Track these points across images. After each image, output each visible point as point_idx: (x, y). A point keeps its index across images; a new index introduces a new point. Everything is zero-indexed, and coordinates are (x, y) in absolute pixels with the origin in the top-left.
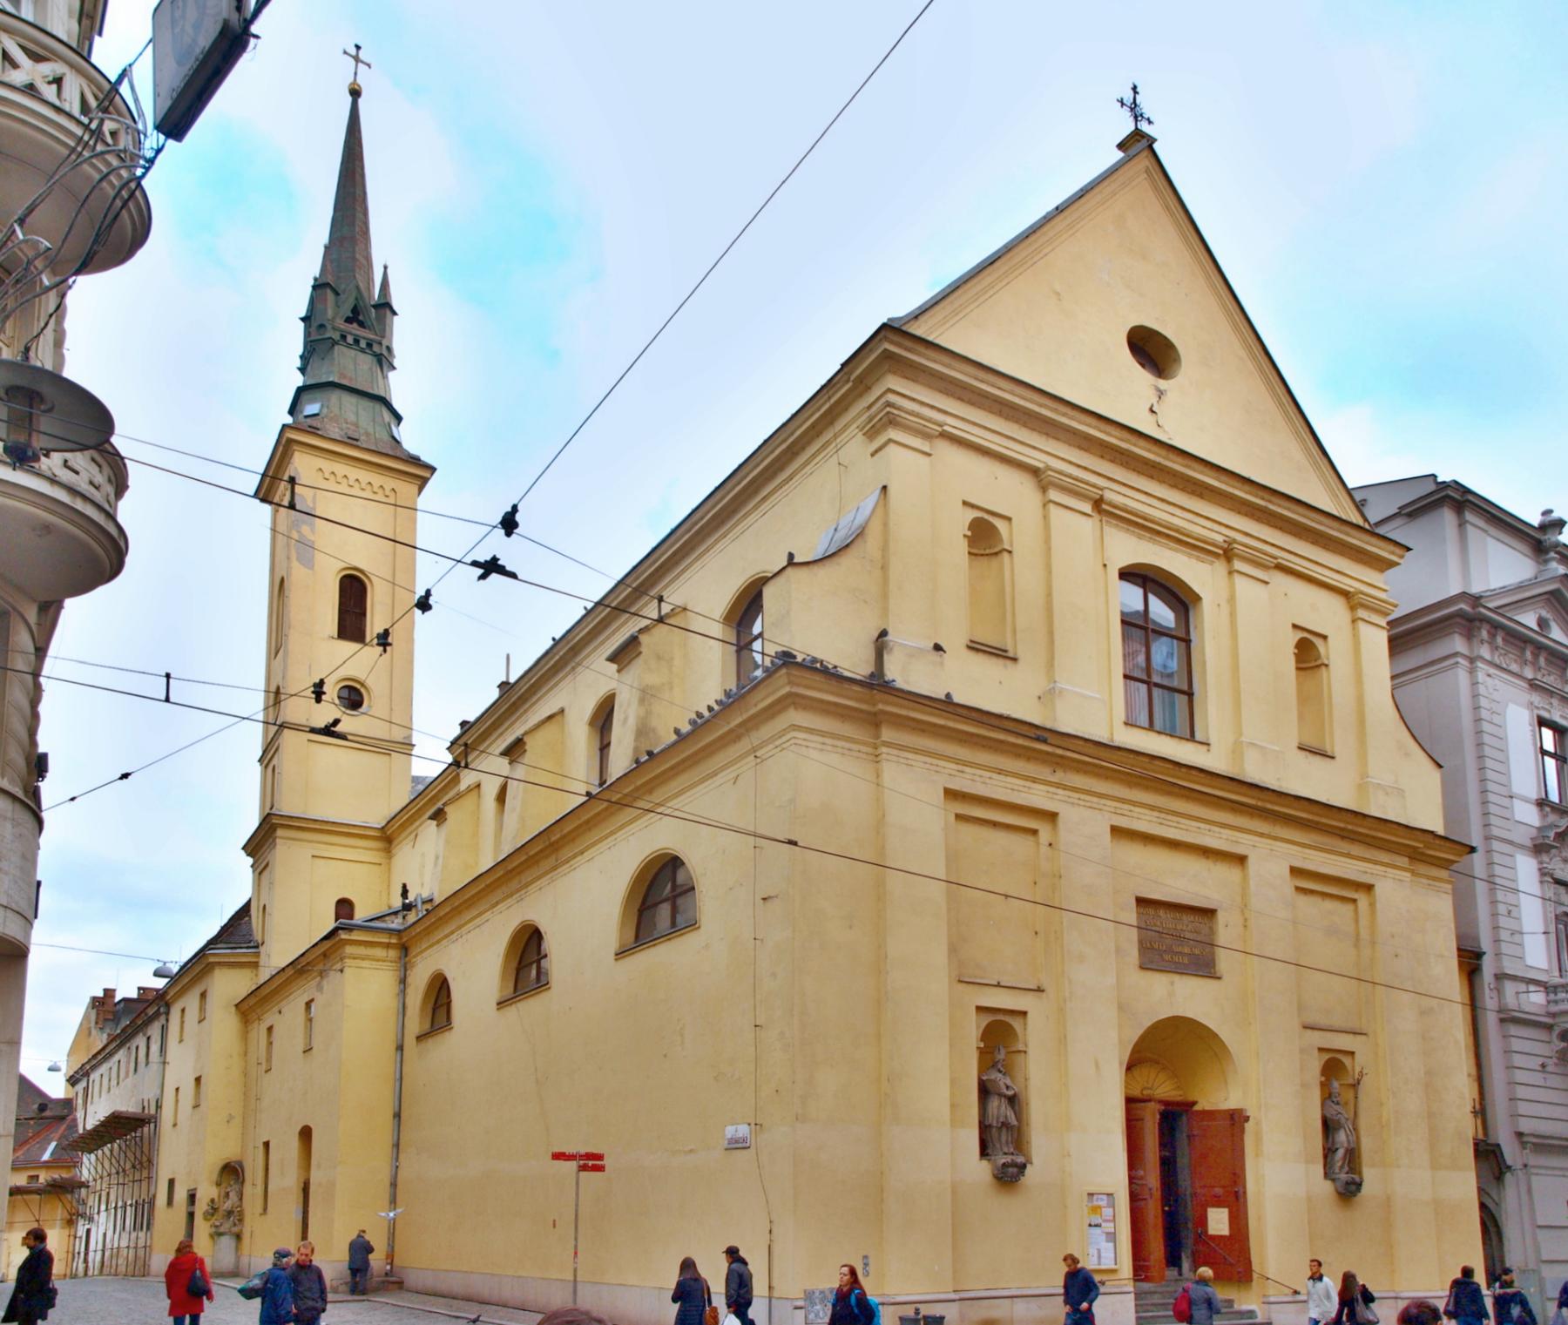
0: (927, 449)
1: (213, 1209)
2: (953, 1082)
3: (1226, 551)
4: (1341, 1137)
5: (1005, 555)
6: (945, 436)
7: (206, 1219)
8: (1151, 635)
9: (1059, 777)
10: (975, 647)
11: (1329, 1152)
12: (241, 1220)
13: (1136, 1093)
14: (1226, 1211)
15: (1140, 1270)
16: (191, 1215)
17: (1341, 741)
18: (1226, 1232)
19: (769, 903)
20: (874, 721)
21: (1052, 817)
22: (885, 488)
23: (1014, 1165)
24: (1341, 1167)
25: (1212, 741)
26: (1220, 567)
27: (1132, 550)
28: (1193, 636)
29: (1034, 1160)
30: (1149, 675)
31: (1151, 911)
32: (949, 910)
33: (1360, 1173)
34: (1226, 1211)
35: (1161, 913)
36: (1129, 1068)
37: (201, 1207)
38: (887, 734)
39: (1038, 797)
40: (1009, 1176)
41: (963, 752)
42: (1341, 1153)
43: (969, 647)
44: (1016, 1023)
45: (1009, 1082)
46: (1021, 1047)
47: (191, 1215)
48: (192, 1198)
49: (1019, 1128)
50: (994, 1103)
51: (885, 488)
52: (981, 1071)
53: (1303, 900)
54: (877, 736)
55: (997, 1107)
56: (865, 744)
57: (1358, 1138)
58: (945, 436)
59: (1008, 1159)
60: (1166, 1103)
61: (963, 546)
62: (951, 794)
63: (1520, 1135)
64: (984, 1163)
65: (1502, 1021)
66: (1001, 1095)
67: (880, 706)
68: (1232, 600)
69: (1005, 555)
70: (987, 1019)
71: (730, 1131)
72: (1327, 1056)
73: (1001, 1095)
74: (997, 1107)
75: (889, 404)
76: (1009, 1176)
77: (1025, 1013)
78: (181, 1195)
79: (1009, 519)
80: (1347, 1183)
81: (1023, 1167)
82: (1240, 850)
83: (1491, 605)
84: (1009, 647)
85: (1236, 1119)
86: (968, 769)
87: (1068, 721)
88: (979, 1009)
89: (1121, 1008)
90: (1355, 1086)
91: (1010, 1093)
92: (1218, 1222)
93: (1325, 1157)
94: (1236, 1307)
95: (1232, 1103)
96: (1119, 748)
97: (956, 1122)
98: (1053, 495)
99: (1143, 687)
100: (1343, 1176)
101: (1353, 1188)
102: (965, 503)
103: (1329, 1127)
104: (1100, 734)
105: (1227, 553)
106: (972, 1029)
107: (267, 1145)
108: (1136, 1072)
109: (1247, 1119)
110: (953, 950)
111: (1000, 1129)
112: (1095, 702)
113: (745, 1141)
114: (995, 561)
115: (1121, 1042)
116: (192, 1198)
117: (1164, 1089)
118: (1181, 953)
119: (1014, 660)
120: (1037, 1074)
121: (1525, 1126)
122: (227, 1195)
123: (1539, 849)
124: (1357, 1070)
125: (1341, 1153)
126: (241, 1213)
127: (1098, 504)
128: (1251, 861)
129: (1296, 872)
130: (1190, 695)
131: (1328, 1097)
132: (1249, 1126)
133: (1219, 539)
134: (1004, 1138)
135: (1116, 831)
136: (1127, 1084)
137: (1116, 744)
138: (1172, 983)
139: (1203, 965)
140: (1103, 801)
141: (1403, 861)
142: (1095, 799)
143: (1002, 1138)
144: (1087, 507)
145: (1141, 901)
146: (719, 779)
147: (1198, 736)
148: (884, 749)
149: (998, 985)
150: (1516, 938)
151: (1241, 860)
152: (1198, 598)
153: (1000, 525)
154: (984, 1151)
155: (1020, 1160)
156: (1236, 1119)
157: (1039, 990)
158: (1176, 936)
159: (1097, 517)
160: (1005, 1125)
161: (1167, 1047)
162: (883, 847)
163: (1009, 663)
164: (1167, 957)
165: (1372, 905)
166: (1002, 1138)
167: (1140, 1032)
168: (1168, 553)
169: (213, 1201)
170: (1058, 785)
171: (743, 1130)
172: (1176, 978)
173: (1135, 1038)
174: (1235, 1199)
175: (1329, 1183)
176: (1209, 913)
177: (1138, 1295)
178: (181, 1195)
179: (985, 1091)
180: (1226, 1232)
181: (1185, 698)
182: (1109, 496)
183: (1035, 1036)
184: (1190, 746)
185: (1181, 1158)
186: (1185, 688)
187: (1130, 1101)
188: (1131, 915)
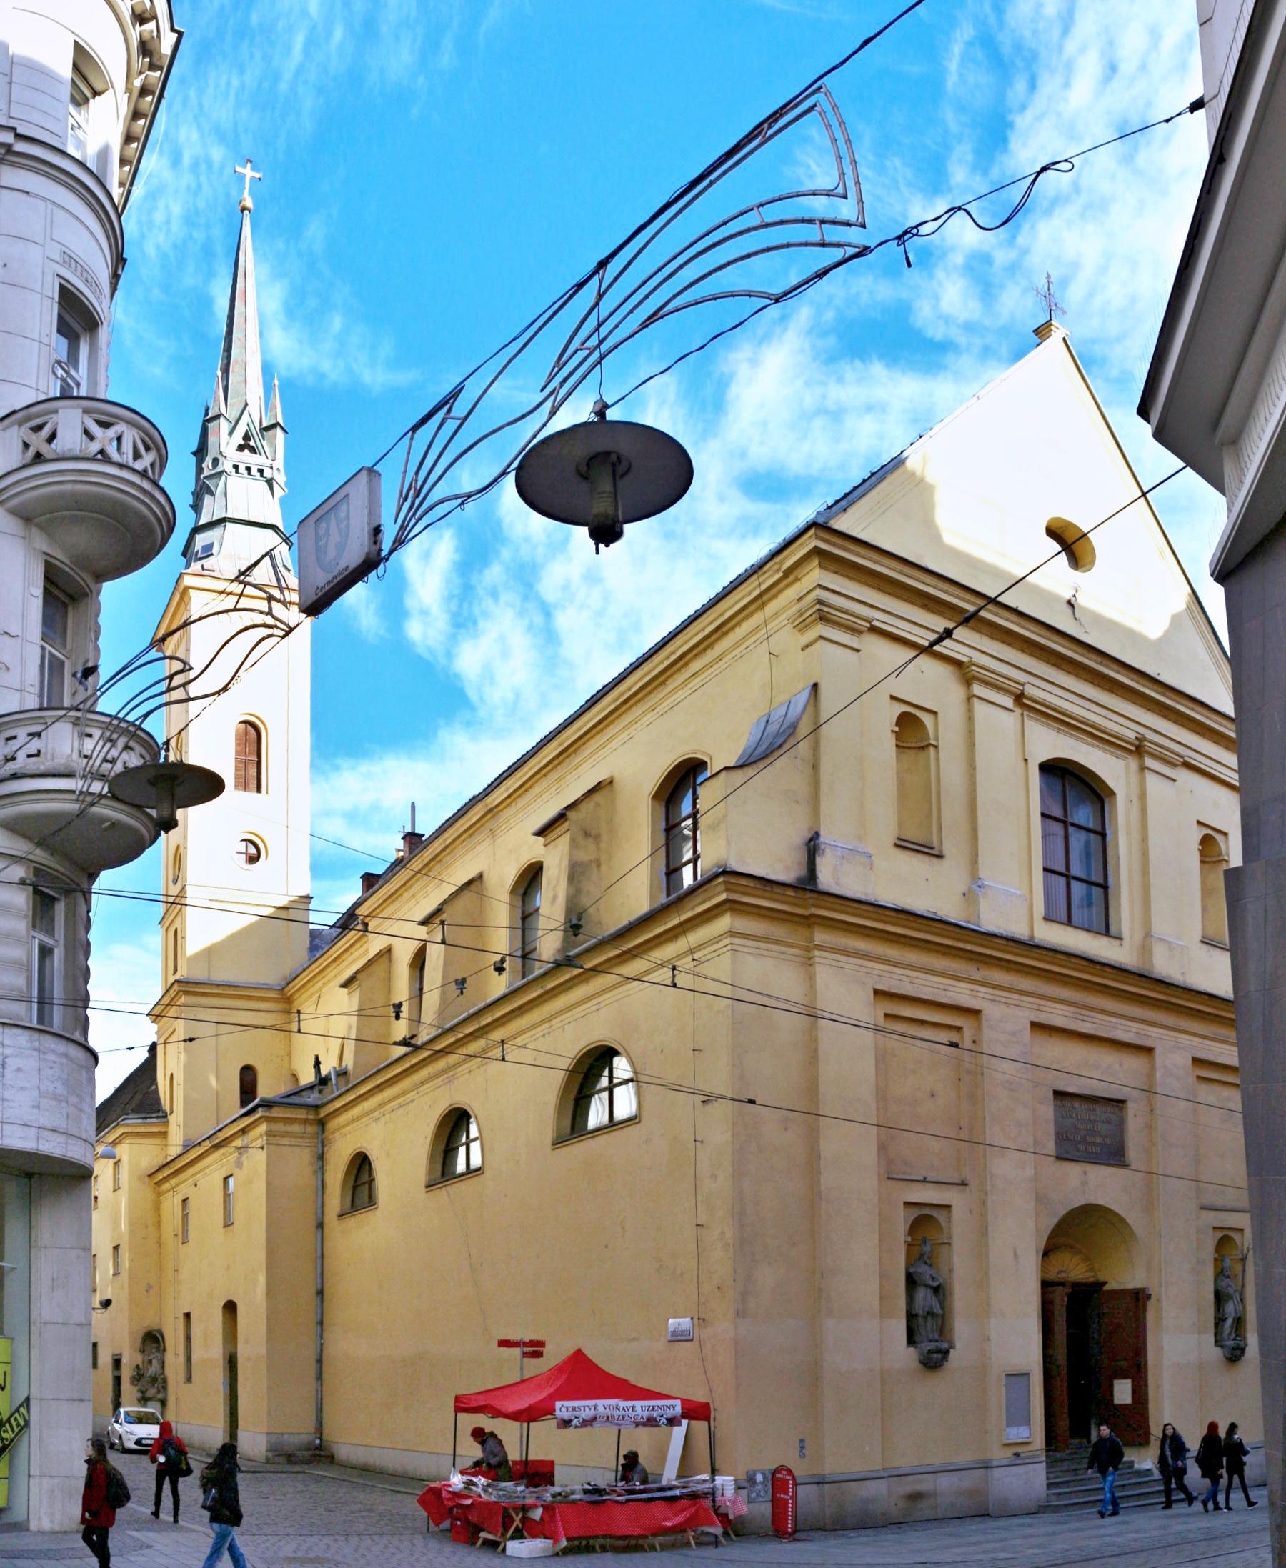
0: (855, 645)
1: (138, 1377)
2: (883, 1276)
3: (1138, 748)
4: (1230, 1308)
5: (932, 749)
6: (874, 630)
7: (132, 1383)
8: (1071, 829)
10: (903, 845)
11: (1219, 1321)
12: (165, 1388)
13: (1052, 1276)
14: (1129, 1381)
15: (1051, 1439)
16: (118, 1380)
18: (1128, 1400)
20: (809, 921)
21: (975, 1013)
22: (815, 686)
23: (939, 1351)
24: (1230, 1334)
25: (1126, 933)
26: (1133, 763)
27: (1051, 744)
28: (1108, 831)
29: (958, 1344)
30: (1068, 868)
31: (1067, 1103)
32: (878, 1109)
33: (1245, 1338)
34: (1129, 1381)
35: (1077, 1105)
36: (1046, 1254)
37: (126, 1374)
38: (821, 936)
39: (962, 994)
40: (934, 1360)
41: (892, 952)
42: (1229, 1322)
43: (896, 845)
44: (940, 1216)
45: (932, 1272)
47: (118, 1380)
48: (117, 1363)
49: (943, 1316)
50: (922, 1294)
51: (815, 686)
52: (909, 1264)
54: (812, 940)
55: (923, 1297)
56: (798, 947)
57: (1244, 1307)
58: (874, 630)
59: (932, 1346)
60: (1075, 1285)
61: (891, 741)
64: (912, 1349)
66: (926, 1286)
67: (814, 911)
68: (1143, 796)
69: (932, 749)
73: (926, 1286)
74: (923, 1297)
75: (820, 602)
76: (934, 1360)
77: (948, 1207)
78: (105, 1359)
79: (935, 713)
80: (1233, 1349)
82: (1148, 1043)
84: (935, 844)
85: (1139, 1298)
86: (897, 970)
87: (991, 920)
88: (906, 1204)
89: (1038, 1198)
91: (935, 1284)
92: (1122, 1392)
93: (1216, 1325)
94: (1136, 1466)
96: (1039, 947)
97: (885, 1313)
98: (978, 689)
99: (1062, 880)
100: (1230, 1343)
101: (1238, 1352)
102: (893, 698)
103: (1220, 1298)
104: (1018, 929)
105: (1138, 749)
106: (901, 1222)
107: (188, 1315)
108: (1052, 1257)
109: (1149, 1297)
111: (925, 1317)
112: (1013, 898)
114: (922, 755)
115: (1037, 1230)
116: (117, 1363)
117: (1074, 1269)
118: (1094, 1144)
119: (940, 856)
120: (959, 1265)
122: (150, 1362)
125: (1229, 1322)
126: (165, 1381)
127: (1019, 698)
128: (1158, 1052)
129: (1197, 1061)
130: (1105, 887)
131: (1220, 1273)
132: (1151, 1305)
133: (1132, 735)
134: (929, 1324)
135: (1036, 1026)
136: (1044, 1268)
137: (1037, 941)
138: (1085, 1173)
139: (1115, 1155)
140: (1024, 998)
142: (1016, 996)
143: (928, 1327)
144: (1008, 702)
145: (1059, 1095)
147: (1113, 929)
148: (817, 953)
149: (925, 1181)
151: (1149, 1050)
152: (1112, 793)
153: (927, 719)
154: (911, 1340)
155: (945, 1345)
156: (1139, 1298)
157: (964, 1184)
158: (1090, 1126)
159: (1018, 711)
160: (931, 1313)
161: (1077, 1229)
162: (816, 1050)
163: (935, 860)
164: (1082, 1148)
166: (928, 1327)
167: (1055, 1220)
168: (1084, 747)
169: (138, 1366)
170: (983, 983)
172: (1088, 1167)
173: (1051, 1227)
174: (1137, 1371)
175: (1218, 1349)
176: (1120, 1103)
177: (1051, 1463)
178: (105, 1359)
179: (912, 1282)
180: (1128, 1400)
181: (1100, 890)
182: (1029, 691)
183: (960, 1227)
184: (1104, 941)
185: (1091, 1336)
186: (1101, 881)
187: (1046, 1285)
188: (1047, 1111)
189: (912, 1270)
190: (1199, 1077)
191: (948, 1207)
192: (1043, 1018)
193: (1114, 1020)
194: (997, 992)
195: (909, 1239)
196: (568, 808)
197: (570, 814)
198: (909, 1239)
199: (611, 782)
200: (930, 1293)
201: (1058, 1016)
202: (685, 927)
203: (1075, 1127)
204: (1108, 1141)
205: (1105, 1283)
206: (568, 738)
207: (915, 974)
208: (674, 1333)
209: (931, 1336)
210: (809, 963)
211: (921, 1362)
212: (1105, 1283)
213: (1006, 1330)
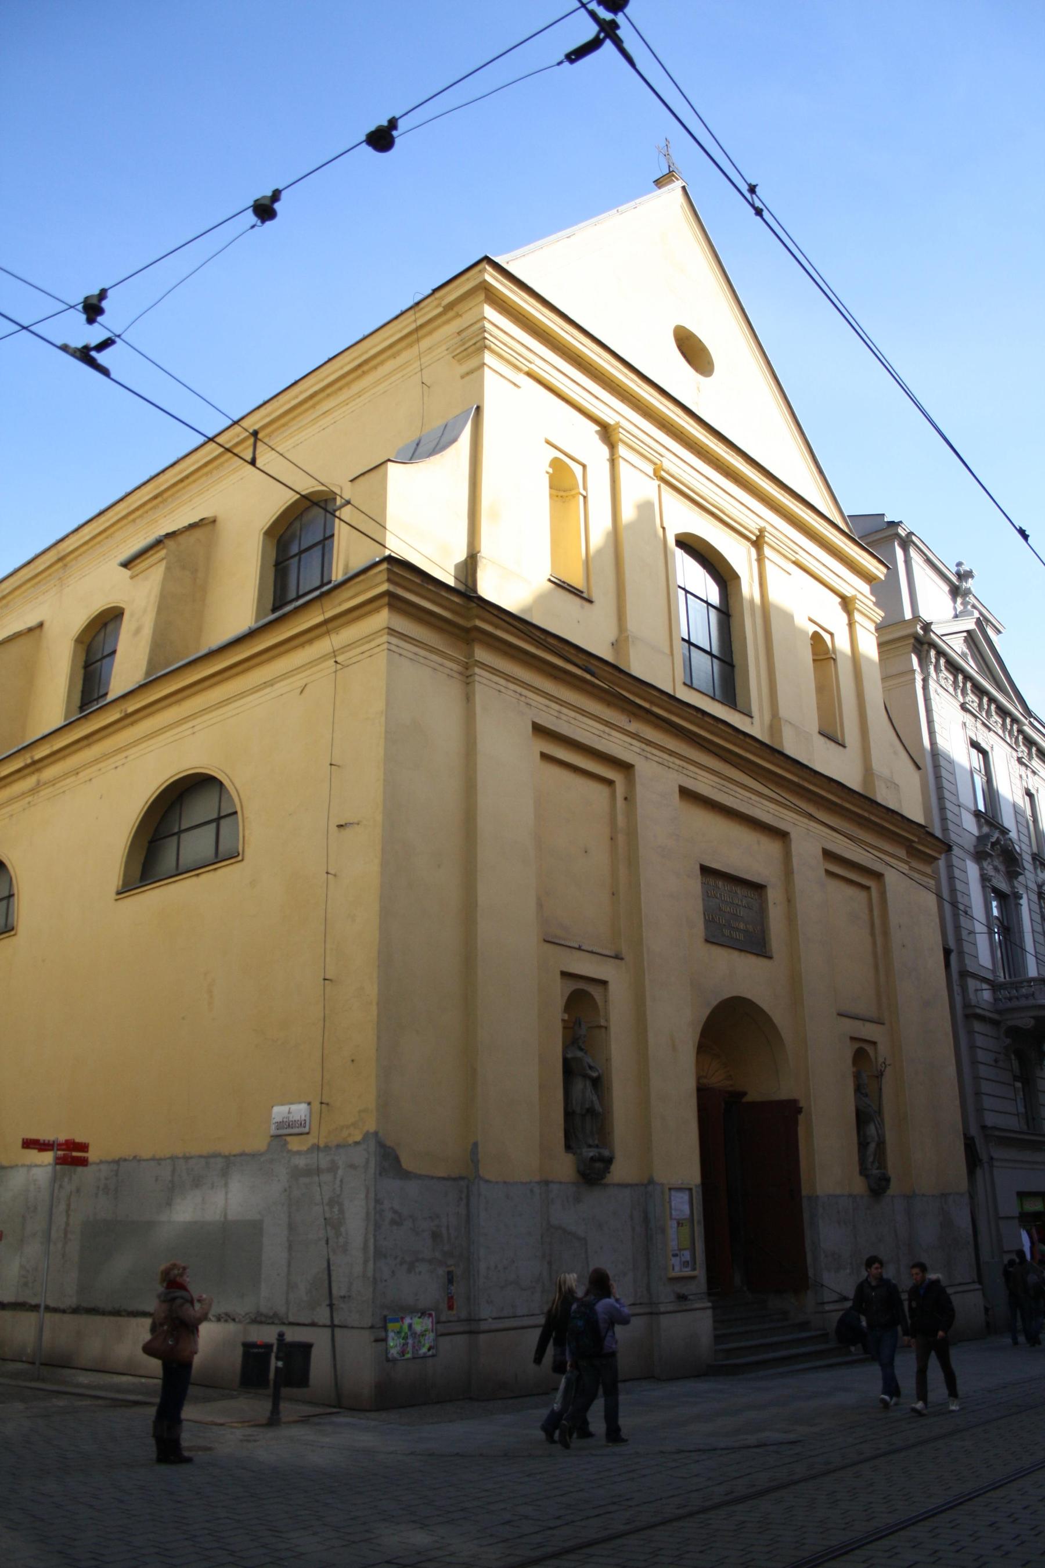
4: (872, 1130)
9: (634, 726)
17: (851, 732)
19: (347, 832)
24: (873, 1162)
31: (711, 881)
35: (720, 884)
38: (481, 654)
44: (595, 992)
45: (590, 1061)
46: (603, 1023)
50: (579, 1085)
53: (833, 885)
59: (592, 1153)
62: (539, 730)
63: (984, 1127)
65: (967, 1017)
66: (586, 1076)
70: (573, 986)
71: (279, 1112)
72: (857, 1045)
73: (586, 1076)
81: (609, 1161)
83: (939, 633)
88: (565, 975)
90: (880, 1075)
91: (595, 1074)
95: (785, 1092)
109: (799, 1110)
110: (540, 905)
113: (302, 1124)
118: (737, 929)
121: (990, 1120)
123: (979, 856)
124: (881, 1060)
129: (828, 854)
132: (801, 1118)
135: (686, 793)
139: (756, 944)
141: (902, 853)
146: (281, 687)
148: (477, 670)
149: (580, 949)
150: (970, 938)
160: (591, 1111)
164: (727, 932)
165: (883, 894)
171: (299, 1111)
176: (758, 888)
179: (570, 1070)
188: (695, 884)
189: (569, 1056)
190: (827, 872)
191: (604, 983)
192: (690, 784)
193: (754, 797)
194: (648, 749)
195: (566, 1017)
196: (168, 536)
197: (170, 543)
198: (566, 1017)
199: (214, 521)
200: (588, 1083)
201: (704, 785)
202: (330, 626)
203: (720, 909)
204: (750, 928)
205: (745, 1094)
206: (167, 481)
207: (572, 714)
208: (280, 1125)
209: (591, 1142)
210: (467, 678)
211: (579, 1171)
212: (745, 1094)
213: (662, 1136)
